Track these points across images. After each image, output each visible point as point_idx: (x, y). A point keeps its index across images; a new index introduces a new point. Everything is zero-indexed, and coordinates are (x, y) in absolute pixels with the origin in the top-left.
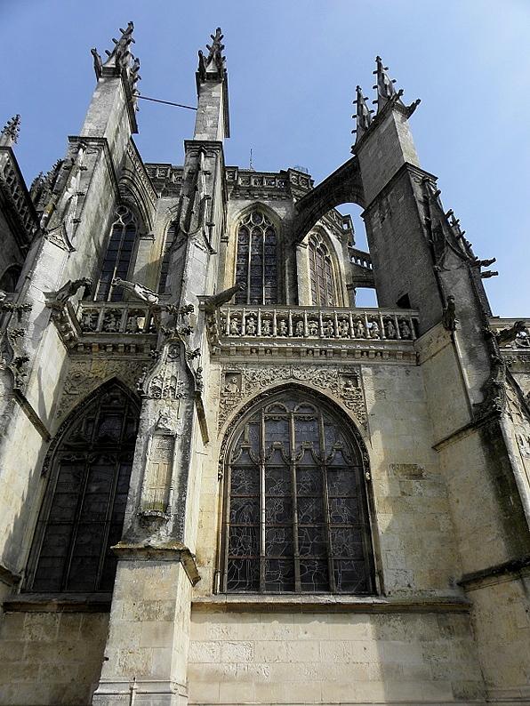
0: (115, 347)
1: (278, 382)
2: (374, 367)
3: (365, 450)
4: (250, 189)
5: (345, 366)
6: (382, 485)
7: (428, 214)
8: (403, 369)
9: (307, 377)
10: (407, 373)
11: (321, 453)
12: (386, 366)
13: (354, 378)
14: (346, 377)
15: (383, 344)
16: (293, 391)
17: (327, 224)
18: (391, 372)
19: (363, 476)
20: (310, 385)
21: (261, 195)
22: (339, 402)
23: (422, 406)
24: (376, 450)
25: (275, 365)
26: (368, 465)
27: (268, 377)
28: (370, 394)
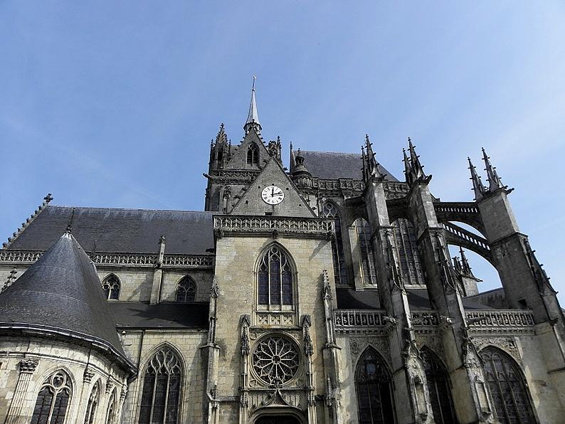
0: (421, 331)
2: (519, 336)
3: (523, 374)
5: (508, 337)
6: (533, 389)
7: (532, 264)
8: (530, 337)
9: (495, 342)
10: (532, 339)
11: (506, 375)
12: (524, 336)
15: (522, 326)
18: (526, 339)
19: (525, 386)
20: (497, 346)
22: (509, 353)
23: (540, 354)
24: (528, 374)
25: (482, 337)
26: (526, 380)
28: (520, 349)
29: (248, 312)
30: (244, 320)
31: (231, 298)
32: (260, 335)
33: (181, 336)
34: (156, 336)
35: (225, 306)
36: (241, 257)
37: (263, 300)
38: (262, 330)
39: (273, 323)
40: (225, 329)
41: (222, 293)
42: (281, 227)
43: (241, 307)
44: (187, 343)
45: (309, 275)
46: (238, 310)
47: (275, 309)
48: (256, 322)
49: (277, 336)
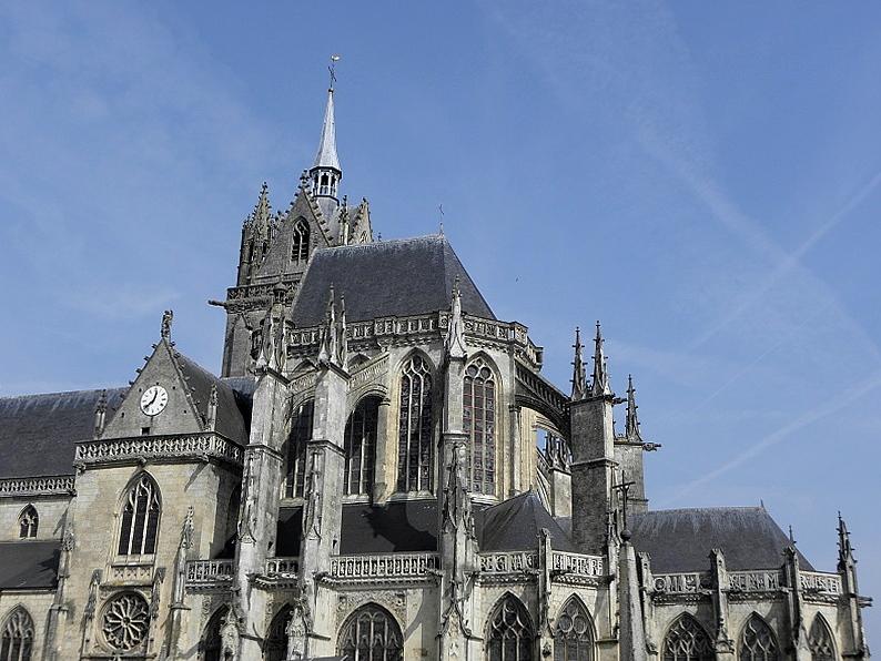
1: (365, 602)
4: (407, 337)
9: (379, 597)
13: (402, 596)
14: (399, 596)
15: (417, 576)
16: (373, 606)
17: (487, 345)
21: (417, 341)
22: (393, 612)
27: (360, 598)
29: (102, 566)
30: (97, 576)
31: (86, 550)
32: (111, 593)
33: (34, 597)
34: (12, 597)
35: (79, 560)
36: (103, 497)
37: (123, 551)
38: (112, 588)
39: (128, 579)
40: (74, 587)
41: (78, 544)
42: (158, 449)
43: (95, 560)
44: (39, 604)
45: (174, 514)
46: (92, 564)
47: (131, 560)
48: (109, 577)
49: (129, 593)
